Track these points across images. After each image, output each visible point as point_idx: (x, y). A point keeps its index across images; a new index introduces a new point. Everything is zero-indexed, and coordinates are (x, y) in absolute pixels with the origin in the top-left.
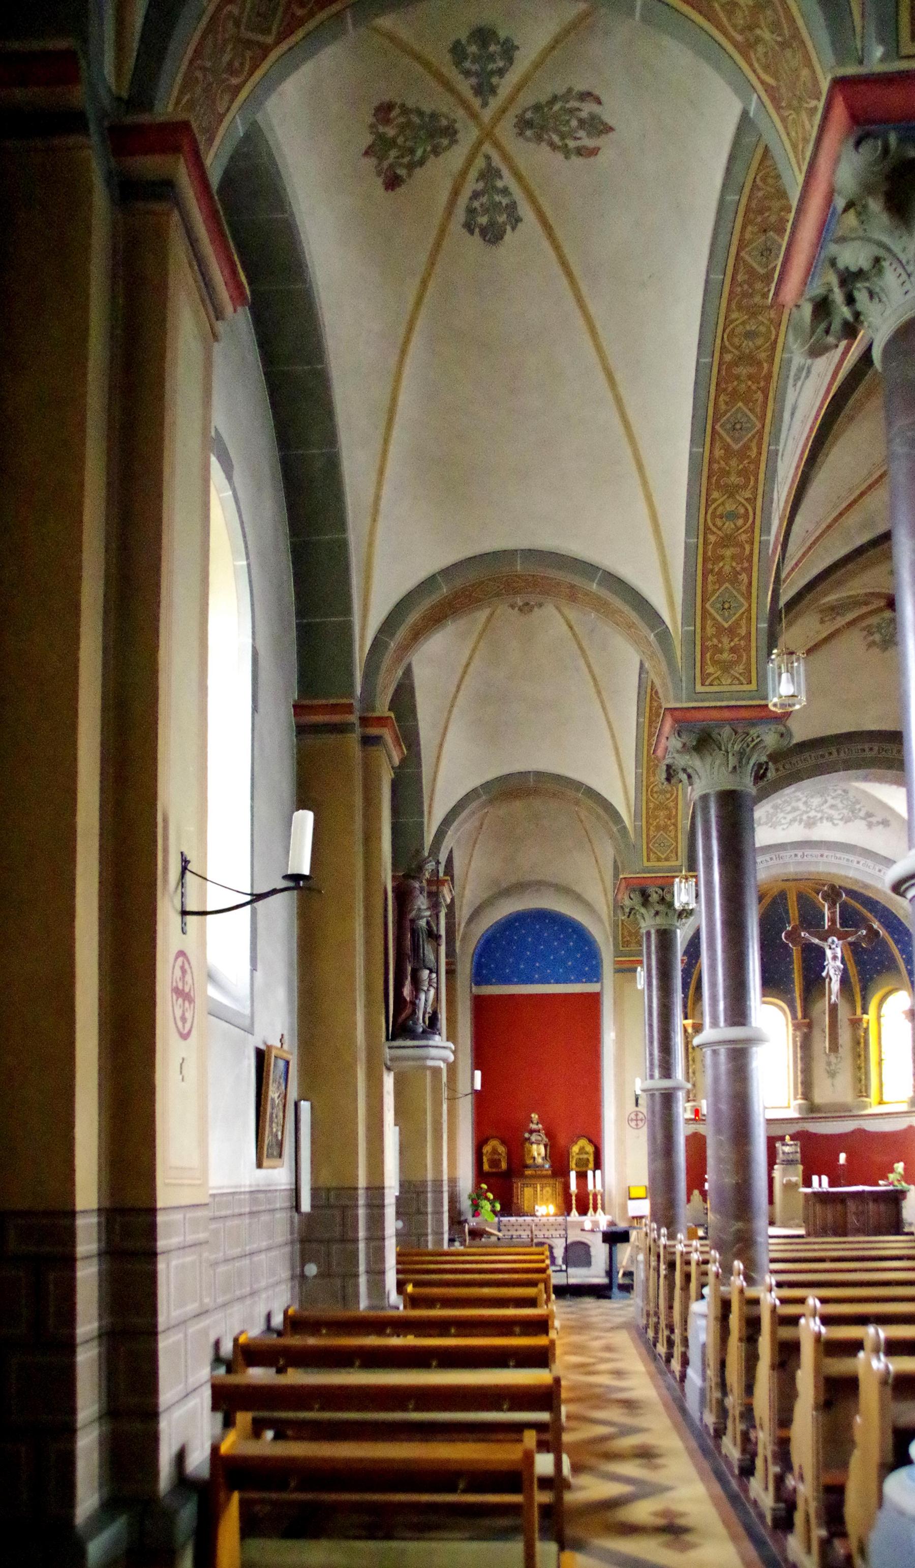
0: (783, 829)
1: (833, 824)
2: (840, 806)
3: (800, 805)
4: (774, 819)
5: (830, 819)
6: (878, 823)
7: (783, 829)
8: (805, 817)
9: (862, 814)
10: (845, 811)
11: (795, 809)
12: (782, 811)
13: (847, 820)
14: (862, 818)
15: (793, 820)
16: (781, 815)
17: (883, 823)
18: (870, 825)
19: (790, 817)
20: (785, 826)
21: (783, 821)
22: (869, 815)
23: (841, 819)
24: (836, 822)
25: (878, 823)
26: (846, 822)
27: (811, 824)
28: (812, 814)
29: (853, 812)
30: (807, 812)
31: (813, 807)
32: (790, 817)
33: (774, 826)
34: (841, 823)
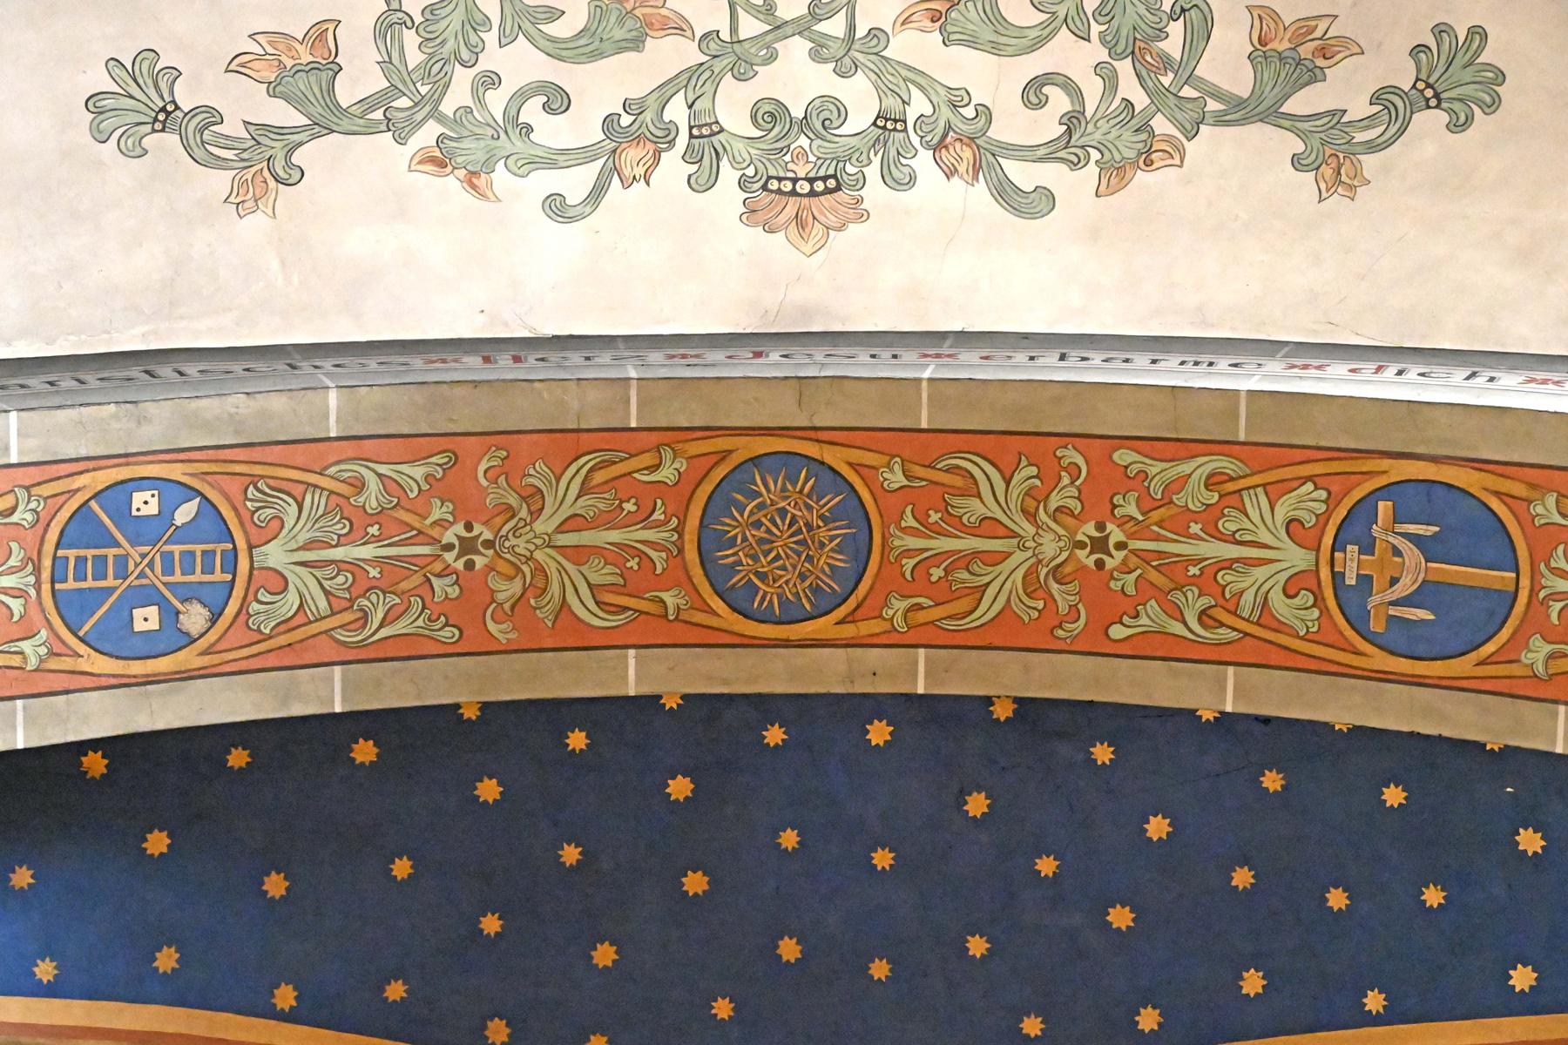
0: (556, 207)
1: (1005, 193)
4: (458, 96)
5: (967, 143)
6: (1394, 108)
7: (556, 207)
8: (733, 107)
9: (1227, 63)
10: (1076, 57)
13: (1119, 149)
14: (1238, 112)
15: (632, 138)
16: (519, 63)
17: (1429, 94)
18: (1333, 156)
19: (602, 88)
20: (576, 182)
21: (550, 131)
22: (1290, 56)
23: (1068, 146)
24: (1022, 174)
25: (1394, 108)
26: (1115, 174)
27: (802, 184)
28: (797, 77)
32: (602, 88)
34: (1073, 185)
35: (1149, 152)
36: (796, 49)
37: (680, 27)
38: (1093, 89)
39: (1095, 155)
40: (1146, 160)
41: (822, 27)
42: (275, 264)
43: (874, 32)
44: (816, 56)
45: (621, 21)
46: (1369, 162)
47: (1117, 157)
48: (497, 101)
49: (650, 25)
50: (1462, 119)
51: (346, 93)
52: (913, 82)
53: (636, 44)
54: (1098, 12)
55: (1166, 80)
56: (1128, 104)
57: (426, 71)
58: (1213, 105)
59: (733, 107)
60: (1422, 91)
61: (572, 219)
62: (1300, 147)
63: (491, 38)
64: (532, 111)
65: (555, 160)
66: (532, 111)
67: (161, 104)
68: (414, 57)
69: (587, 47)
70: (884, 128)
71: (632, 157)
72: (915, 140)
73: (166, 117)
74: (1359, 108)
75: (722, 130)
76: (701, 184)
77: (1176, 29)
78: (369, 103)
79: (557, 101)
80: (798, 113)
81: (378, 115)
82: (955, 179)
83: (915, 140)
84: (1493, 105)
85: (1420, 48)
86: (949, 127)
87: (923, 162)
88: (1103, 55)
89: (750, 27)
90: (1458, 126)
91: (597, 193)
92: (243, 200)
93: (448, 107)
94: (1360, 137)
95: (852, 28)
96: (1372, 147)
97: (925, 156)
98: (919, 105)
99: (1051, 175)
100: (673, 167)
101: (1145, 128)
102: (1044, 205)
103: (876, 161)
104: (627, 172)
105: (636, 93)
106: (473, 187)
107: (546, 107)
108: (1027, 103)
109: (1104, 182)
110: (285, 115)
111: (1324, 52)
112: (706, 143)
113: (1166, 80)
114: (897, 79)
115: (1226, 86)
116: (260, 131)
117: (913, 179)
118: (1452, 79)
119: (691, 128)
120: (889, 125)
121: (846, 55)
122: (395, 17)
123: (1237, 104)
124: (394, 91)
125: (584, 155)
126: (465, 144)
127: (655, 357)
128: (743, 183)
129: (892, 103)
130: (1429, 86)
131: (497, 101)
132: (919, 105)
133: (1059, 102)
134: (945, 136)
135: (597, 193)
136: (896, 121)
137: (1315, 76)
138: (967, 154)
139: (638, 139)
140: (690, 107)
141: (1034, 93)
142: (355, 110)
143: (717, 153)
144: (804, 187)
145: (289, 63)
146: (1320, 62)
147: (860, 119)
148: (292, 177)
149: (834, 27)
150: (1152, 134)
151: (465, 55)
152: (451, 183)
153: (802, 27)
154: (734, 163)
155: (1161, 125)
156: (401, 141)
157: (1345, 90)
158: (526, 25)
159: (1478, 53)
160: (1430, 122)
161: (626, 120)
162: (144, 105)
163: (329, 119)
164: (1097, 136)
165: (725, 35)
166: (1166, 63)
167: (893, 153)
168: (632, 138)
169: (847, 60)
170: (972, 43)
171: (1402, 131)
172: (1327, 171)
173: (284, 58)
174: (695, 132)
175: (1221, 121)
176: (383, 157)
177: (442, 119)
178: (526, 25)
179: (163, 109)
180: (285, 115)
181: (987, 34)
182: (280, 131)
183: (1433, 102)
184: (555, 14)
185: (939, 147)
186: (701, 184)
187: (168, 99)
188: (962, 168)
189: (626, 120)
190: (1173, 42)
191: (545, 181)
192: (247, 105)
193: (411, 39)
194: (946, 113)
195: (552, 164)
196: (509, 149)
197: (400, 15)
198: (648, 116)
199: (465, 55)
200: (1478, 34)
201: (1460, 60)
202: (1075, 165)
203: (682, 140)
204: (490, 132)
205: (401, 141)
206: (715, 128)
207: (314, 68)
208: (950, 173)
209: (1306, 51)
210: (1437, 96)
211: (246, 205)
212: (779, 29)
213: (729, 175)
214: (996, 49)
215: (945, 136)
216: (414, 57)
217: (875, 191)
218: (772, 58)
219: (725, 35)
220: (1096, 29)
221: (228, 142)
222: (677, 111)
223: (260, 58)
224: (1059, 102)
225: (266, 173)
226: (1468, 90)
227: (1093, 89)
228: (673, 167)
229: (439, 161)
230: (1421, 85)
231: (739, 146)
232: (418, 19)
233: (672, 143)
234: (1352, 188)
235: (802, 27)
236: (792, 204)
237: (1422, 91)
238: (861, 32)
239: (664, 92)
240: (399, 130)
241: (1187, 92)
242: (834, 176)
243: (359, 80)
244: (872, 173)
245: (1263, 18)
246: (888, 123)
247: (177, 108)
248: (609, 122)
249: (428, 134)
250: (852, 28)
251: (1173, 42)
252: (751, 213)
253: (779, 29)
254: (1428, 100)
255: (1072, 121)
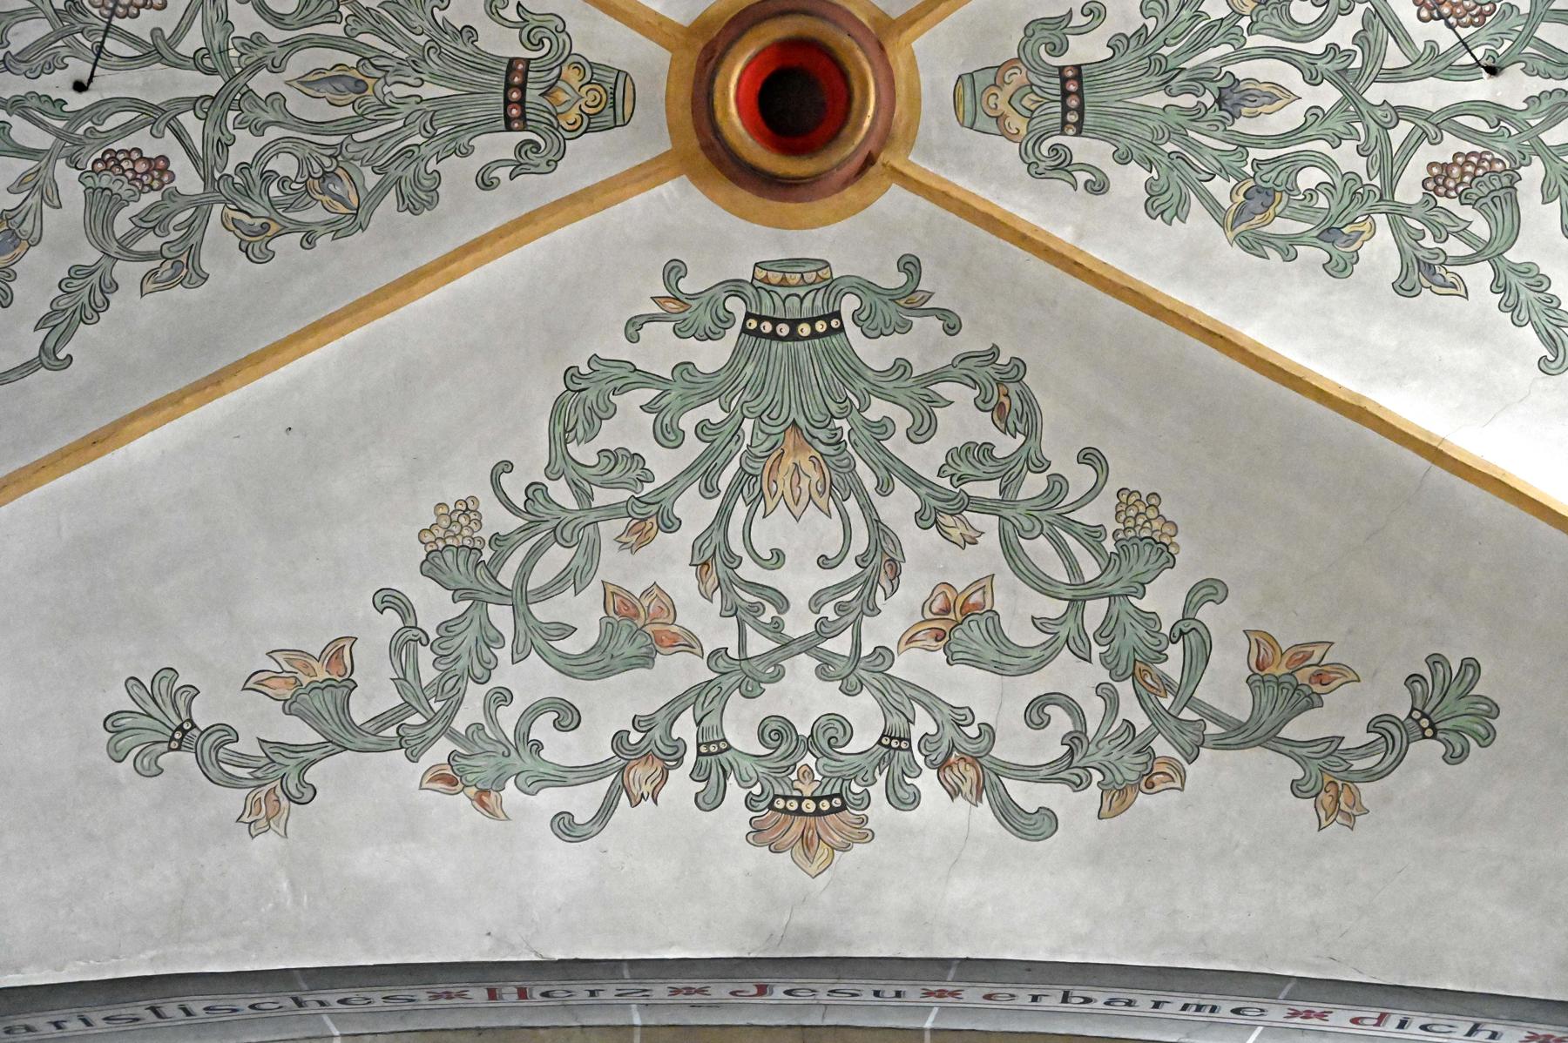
0: (565, 826)
1: (1007, 813)
2: (1020, 611)
3: (668, 568)
4: (470, 713)
5: (970, 763)
6: (1391, 737)
7: (565, 826)
8: (740, 727)
9: (1226, 687)
10: (1079, 677)
11: (637, 632)
12: (539, 639)
14: (1238, 736)
15: (641, 756)
16: (530, 679)
17: (1426, 724)
18: (1331, 783)
19: (613, 705)
20: (583, 801)
21: (560, 748)
23: (1069, 768)
24: (1024, 794)
25: (1391, 737)
26: (1117, 797)
27: (808, 805)
28: (804, 695)
29: (1136, 668)
30: (746, 675)
31: (798, 624)
32: (613, 705)
33: (475, 775)
35: (1150, 774)
36: (805, 665)
37: (689, 644)
38: (1094, 709)
39: (1097, 776)
40: (1147, 782)
41: (828, 645)
42: (285, 885)
43: (881, 651)
44: (823, 674)
45: (632, 638)
46: (1367, 790)
47: (1119, 778)
48: (508, 718)
49: (659, 641)
50: (1458, 750)
51: (360, 712)
52: (918, 701)
53: (646, 660)
54: (1099, 633)
55: (1167, 702)
56: (1130, 725)
57: (439, 686)
58: (1212, 729)
59: (740, 727)
60: (1418, 721)
61: (582, 838)
62: (1299, 773)
63: (504, 654)
64: (543, 729)
65: (563, 777)
66: (543, 729)
67: (178, 723)
68: (428, 674)
69: (599, 664)
70: (889, 746)
71: (640, 774)
72: (920, 759)
73: (182, 735)
74: (1356, 736)
75: (729, 748)
76: (709, 802)
77: (1175, 651)
78: (382, 721)
79: (568, 717)
80: (804, 731)
81: (391, 732)
82: (959, 799)
83: (920, 759)
84: (1487, 739)
85: (1413, 678)
86: (953, 746)
87: (927, 782)
88: (1104, 676)
89: (758, 644)
90: (1455, 757)
91: (607, 809)
92: (255, 821)
93: (460, 724)
94: (1358, 765)
95: (857, 645)
96: (1371, 775)
97: (930, 775)
98: (923, 724)
99: (1053, 796)
100: (681, 785)
101: (1146, 749)
102: (1046, 826)
103: (881, 780)
104: (635, 790)
105: (646, 711)
106: (483, 804)
107: (557, 724)
108: (1029, 723)
109: (1107, 804)
110: (299, 732)
111: (1319, 678)
112: (714, 760)
113: (1167, 702)
114: (900, 697)
115: (1224, 707)
116: (275, 749)
117: (916, 798)
118: (1446, 710)
119: (699, 745)
120: (894, 744)
121: (850, 674)
122: (410, 635)
123: (1240, 727)
124: (407, 707)
125: (592, 772)
126: (479, 761)
127: (660, 991)
128: (750, 802)
129: (897, 721)
130: (1424, 716)
131: (508, 718)
132: (923, 724)
133: (1061, 722)
134: (949, 755)
135: (607, 809)
136: (900, 739)
137: (1313, 701)
138: (971, 773)
139: (648, 756)
140: (698, 724)
141: (1036, 712)
142: (370, 728)
143: (724, 771)
144: (809, 806)
145: (305, 680)
146: (1317, 688)
147: (864, 739)
148: (305, 795)
149: (840, 645)
150: (1153, 757)
151: (478, 671)
152: (462, 801)
153: (809, 645)
154: (741, 782)
155: (1161, 747)
156: (413, 758)
157: (1342, 717)
158: (539, 642)
159: (1472, 684)
160: (1427, 751)
161: (635, 737)
162: (160, 725)
163: (342, 736)
164: (1099, 757)
165: (733, 653)
166: (1166, 685)
167: (898, 772)
168: (641, 756)
169: (853, 679)
170: (976, 662)
171: (1399, 760)
172: (1326, 798)
173: (300, 675)
174: (703, 749)
175: (1221, 744)
176: (394, 775)
177: (454, 736)
178: (539, 642)
179: (180, 728)
180: (299, 732)
181: (990, 654)
182: (294, 749)
183: (1429, 733)
184: (567, 631)
185: (942, 767)
186: (709, 802)
187: (184, 716)
188: (965, 788)
189: (635, 737)
190: (1172, 667)
191: (552, 800)
192: (265, 722)
193: (425, 656)
194: (949, 731)
195: (561, 782)
196: (519, 766)
197: (415, 632)
198: (657, 733)
199: (478, 671)
200: (1471, 665)
201: (1454, 692)
202: (1077, 786)
203: (690, 757)
204: (501, 749)
205: (413, 758)
206: (723, 746)
207: (329, 685)
208: (954, 793)
209: (1303, 676)
210: (1432, 726)
211: (259, 824)
212: (787, 646)
213: (735, 793)
214: (999, 669)
215: (949, 755)
216: (428, 674)
217: (880, 811)
218: (778, 676)
219: (733, 653)
220: (1097, 650)
221: (242, 760)
222: (685, 728)
223: (276, 676)
224: (1061, 722)
225: (279, 791)
226: (1461, 721)
227: (1094, 709)
228: (681, 785)
229: (448, 779)
230: (1416, 715)
231: (746, 763)
232: (433, 636)
233: (680, 761)
234: (1351, 817)
235: (809, 645)
236: (798, 824)
237: (1418, 721)
238: (866, 650)
239: (673, 708)
240: (413, 747)
241: (1187, 714)
242: (839, 795)
243: (374, 696)
244: (877, 791)
245: (1260, 641)
246: (893, 741)
247: (194, 726)
248: (619, 738)
249: (440, 751)
250: (857, 645)
251: (1172, 667)
252: (757, 832)
253: (787, 646)
254: (1424, 730)
255: (1074, 741)
